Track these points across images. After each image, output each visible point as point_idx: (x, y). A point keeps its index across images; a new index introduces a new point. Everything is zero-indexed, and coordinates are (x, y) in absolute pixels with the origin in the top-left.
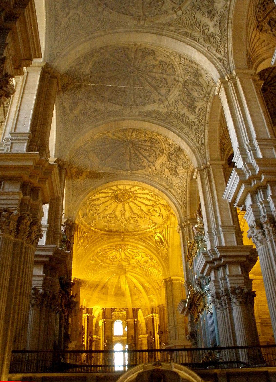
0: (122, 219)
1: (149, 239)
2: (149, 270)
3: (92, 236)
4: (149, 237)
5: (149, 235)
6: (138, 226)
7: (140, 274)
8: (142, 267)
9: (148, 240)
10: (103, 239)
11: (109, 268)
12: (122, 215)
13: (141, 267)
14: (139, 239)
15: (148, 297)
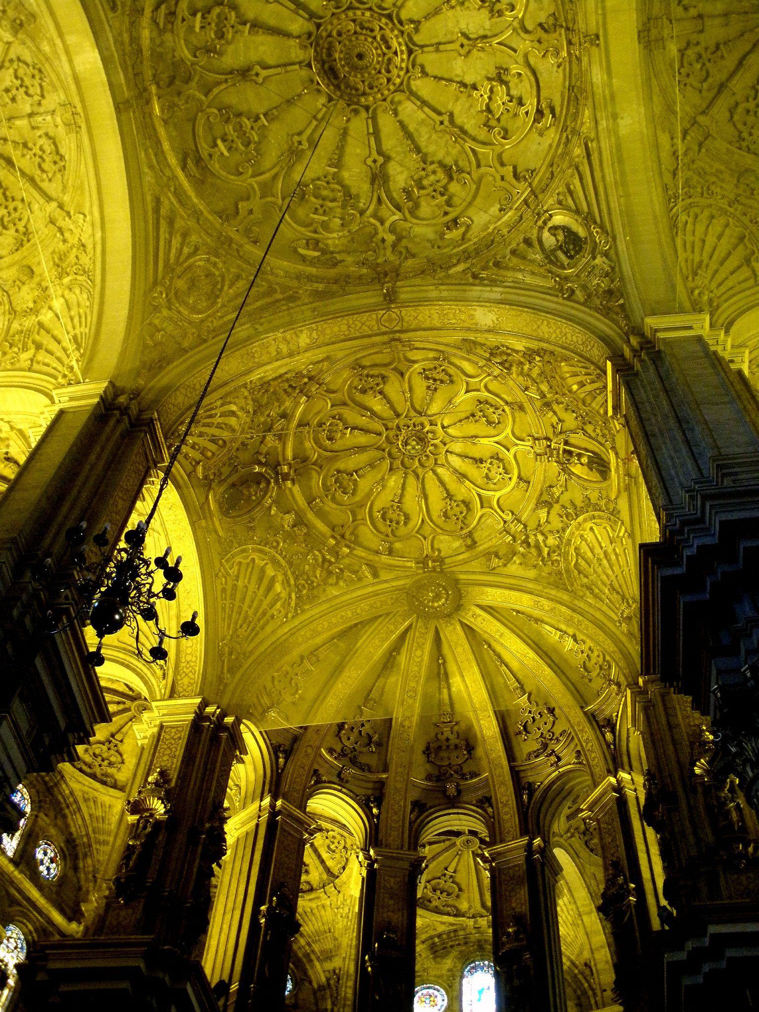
0: (380, 201)
1: (515, 260)
2: (569, 541)
3: (238, 277)
4: (513, 252)
5: (514, 245)
6: (455, 221)
7: (530, 585)
8: (532, 540)
9: (514, 269)
10: (292, 298)
11: (375, 575)
12: (373, 182)
13: (526, 543)
14: (471, 280)
15: (585, 713)
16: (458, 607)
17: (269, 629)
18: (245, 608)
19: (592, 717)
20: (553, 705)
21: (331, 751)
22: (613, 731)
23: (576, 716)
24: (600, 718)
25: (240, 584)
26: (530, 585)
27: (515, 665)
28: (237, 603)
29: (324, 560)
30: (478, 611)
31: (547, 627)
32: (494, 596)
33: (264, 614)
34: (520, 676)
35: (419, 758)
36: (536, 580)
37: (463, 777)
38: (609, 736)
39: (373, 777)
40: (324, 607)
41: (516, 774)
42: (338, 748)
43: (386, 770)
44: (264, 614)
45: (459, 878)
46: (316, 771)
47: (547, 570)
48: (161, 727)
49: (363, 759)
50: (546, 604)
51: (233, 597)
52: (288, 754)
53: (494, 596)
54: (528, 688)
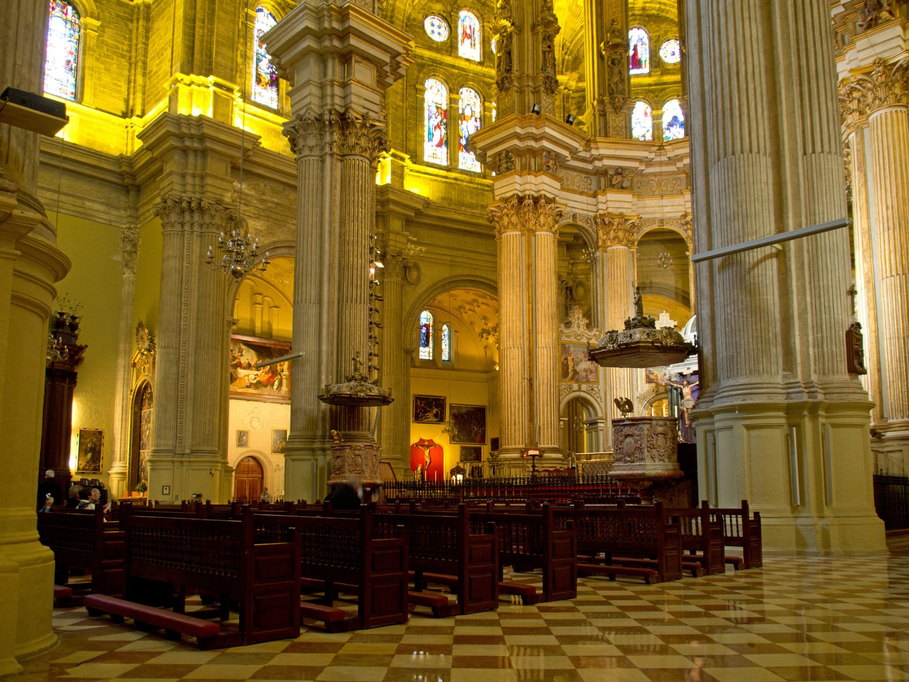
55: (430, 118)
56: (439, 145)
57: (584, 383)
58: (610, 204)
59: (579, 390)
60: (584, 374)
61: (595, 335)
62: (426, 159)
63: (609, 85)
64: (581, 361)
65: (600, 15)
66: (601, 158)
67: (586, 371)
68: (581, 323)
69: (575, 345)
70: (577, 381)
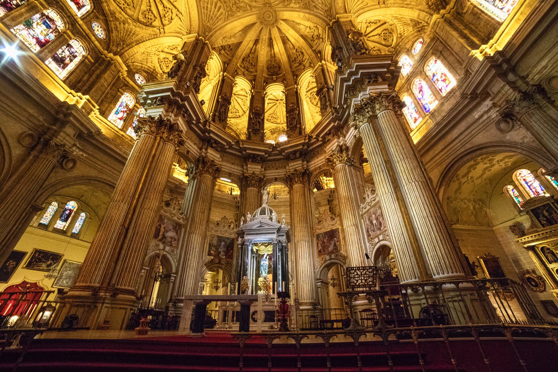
7: (297, 9)
16: (276, 21)
17: (219, 23)
18: (211, 15)
19: (314, 51)
20: (304, 51)
21: (241, 66)
22: (320, 54)
23: (310, 51)
24: (317, 51)
25: (209, 6)
26: (297, 9)
27: (293, 40)
28: (209, 13)
29: (235, 2)
30: (282, 22)
31: (302, 26)
32: (287, 15)
33: (218, 18)
34: (294, 44)
35: (265, 69)
36: (299, 8)
37: (278, 75)
38: (319, 55)
39: (253, 74)
40: (236, 18)
41: (293, 72)
42: (243, 66)
43: (256, 72)
44: (218, 18)
45: (278, 114)
46: (236, 71)
47: (302, 3)
48: (185, 43)
49: (251, 70)
50: (302, 14)
51: (207, 10)
52: (228, 64)
53: (287, 15)
54: (296, 48)
55: (120, 106)
56: (121, 119)
57: (168, 246)
58: (208, 154)
59: (164, 249)
60: (170, 240)
61: (183, 218)
62: (108, 119)
63: (219, 111)
64: (170, 230)
65: (221, 90)
66: (210, 132)
67: (171, 238)
68: (176, 207)
69: (169, 219)
70: (164, 243)
